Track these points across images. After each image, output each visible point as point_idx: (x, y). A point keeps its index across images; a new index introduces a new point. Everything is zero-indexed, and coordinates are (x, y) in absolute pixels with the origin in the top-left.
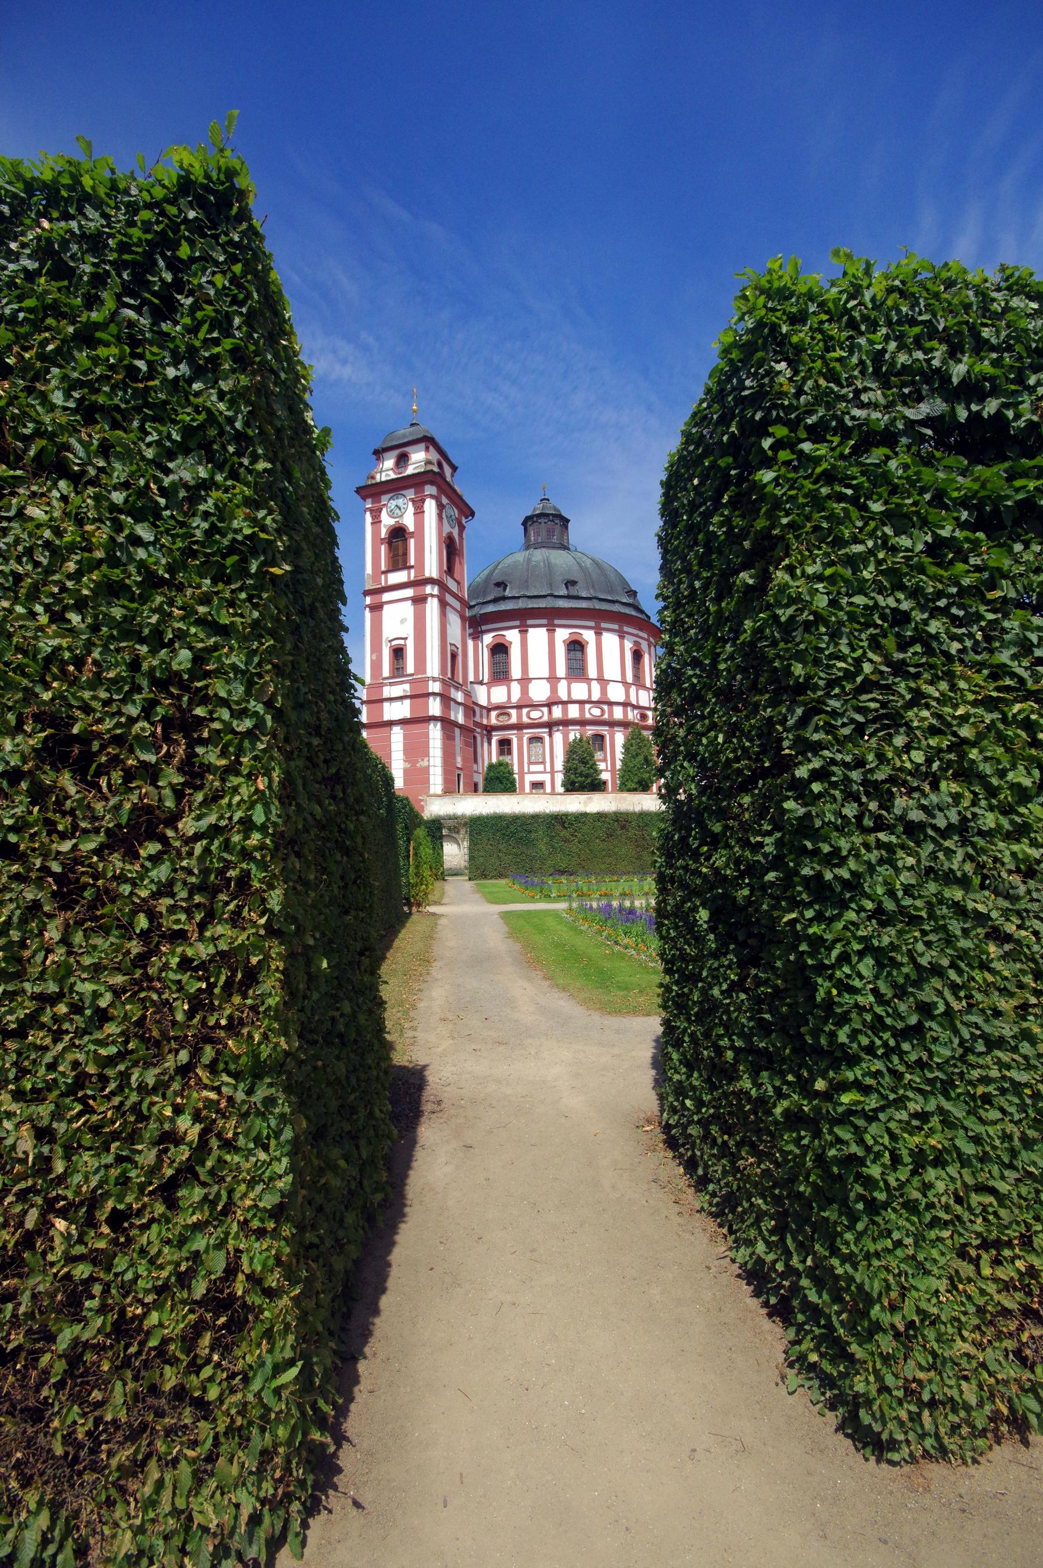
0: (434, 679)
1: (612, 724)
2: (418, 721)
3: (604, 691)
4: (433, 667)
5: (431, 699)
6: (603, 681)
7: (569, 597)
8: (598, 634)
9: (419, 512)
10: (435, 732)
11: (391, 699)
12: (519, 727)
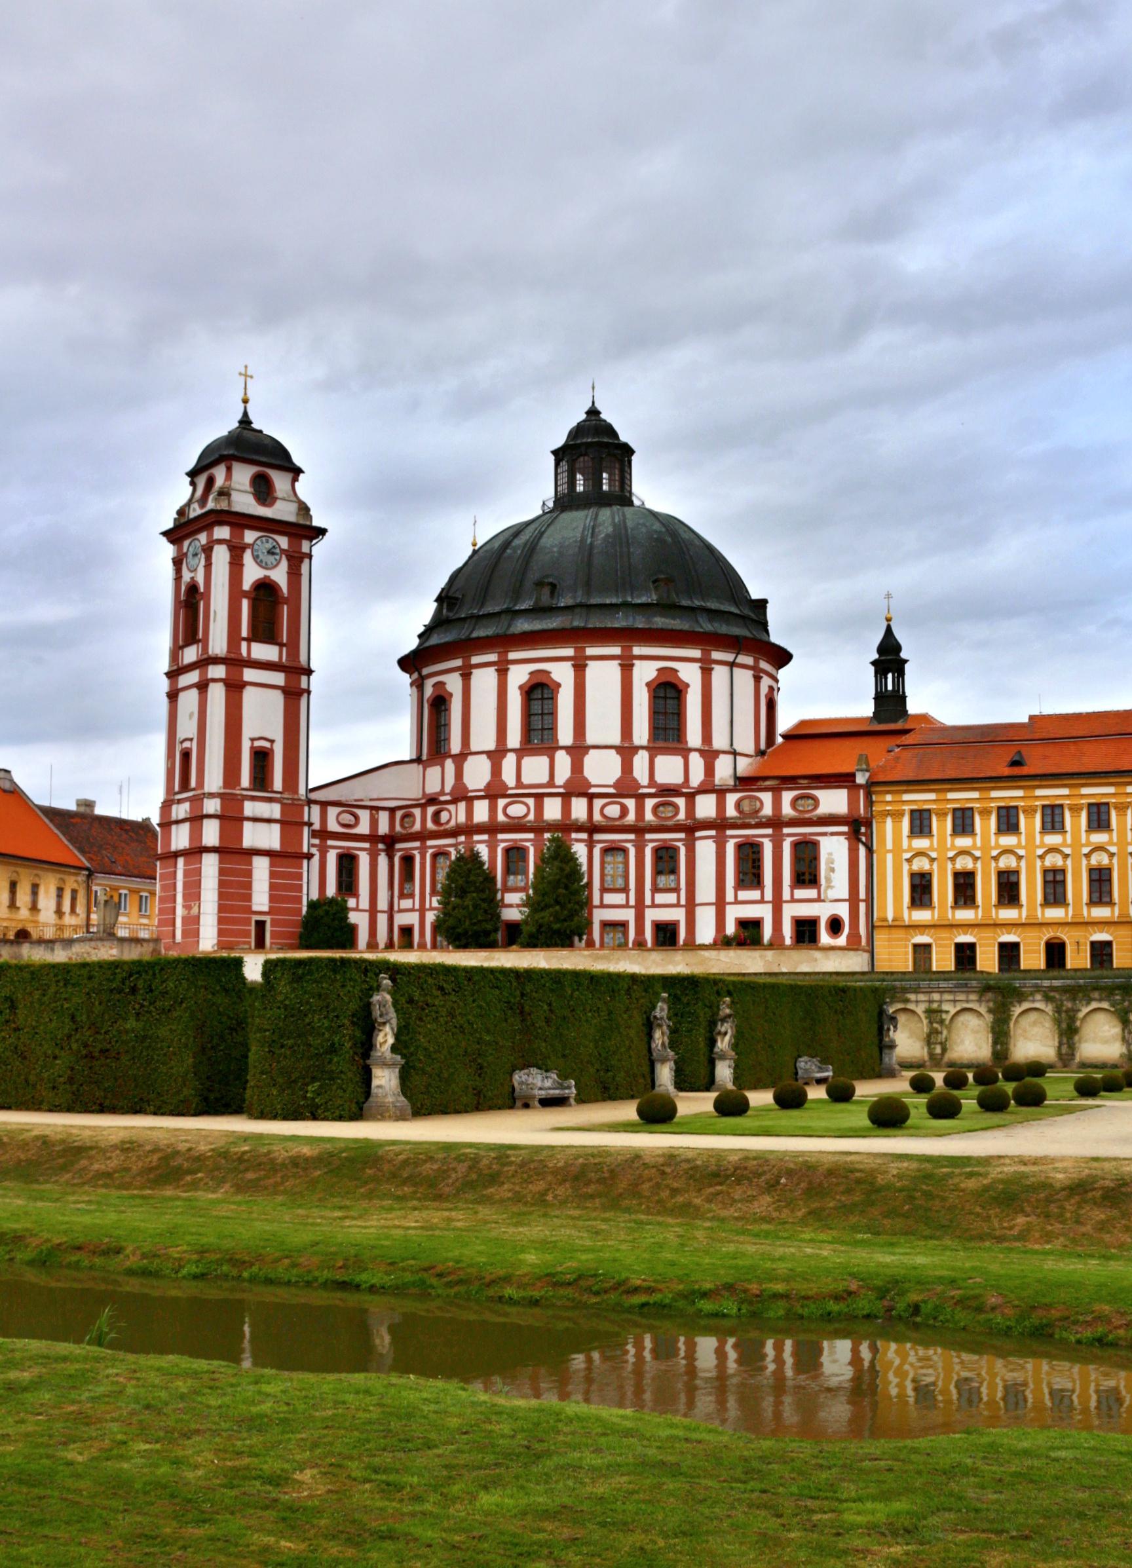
0: (212, 795)
1: (539, 828)
2: (196, 851)
3: (577, 767)
4: (214, 780)
5: (206, 822)
6: (578, 750)
7: (538, 611)
8: (580, 667)
9: (208, 566)
10: (210, 865)
11: (178, 822)
12: (423, 836)
